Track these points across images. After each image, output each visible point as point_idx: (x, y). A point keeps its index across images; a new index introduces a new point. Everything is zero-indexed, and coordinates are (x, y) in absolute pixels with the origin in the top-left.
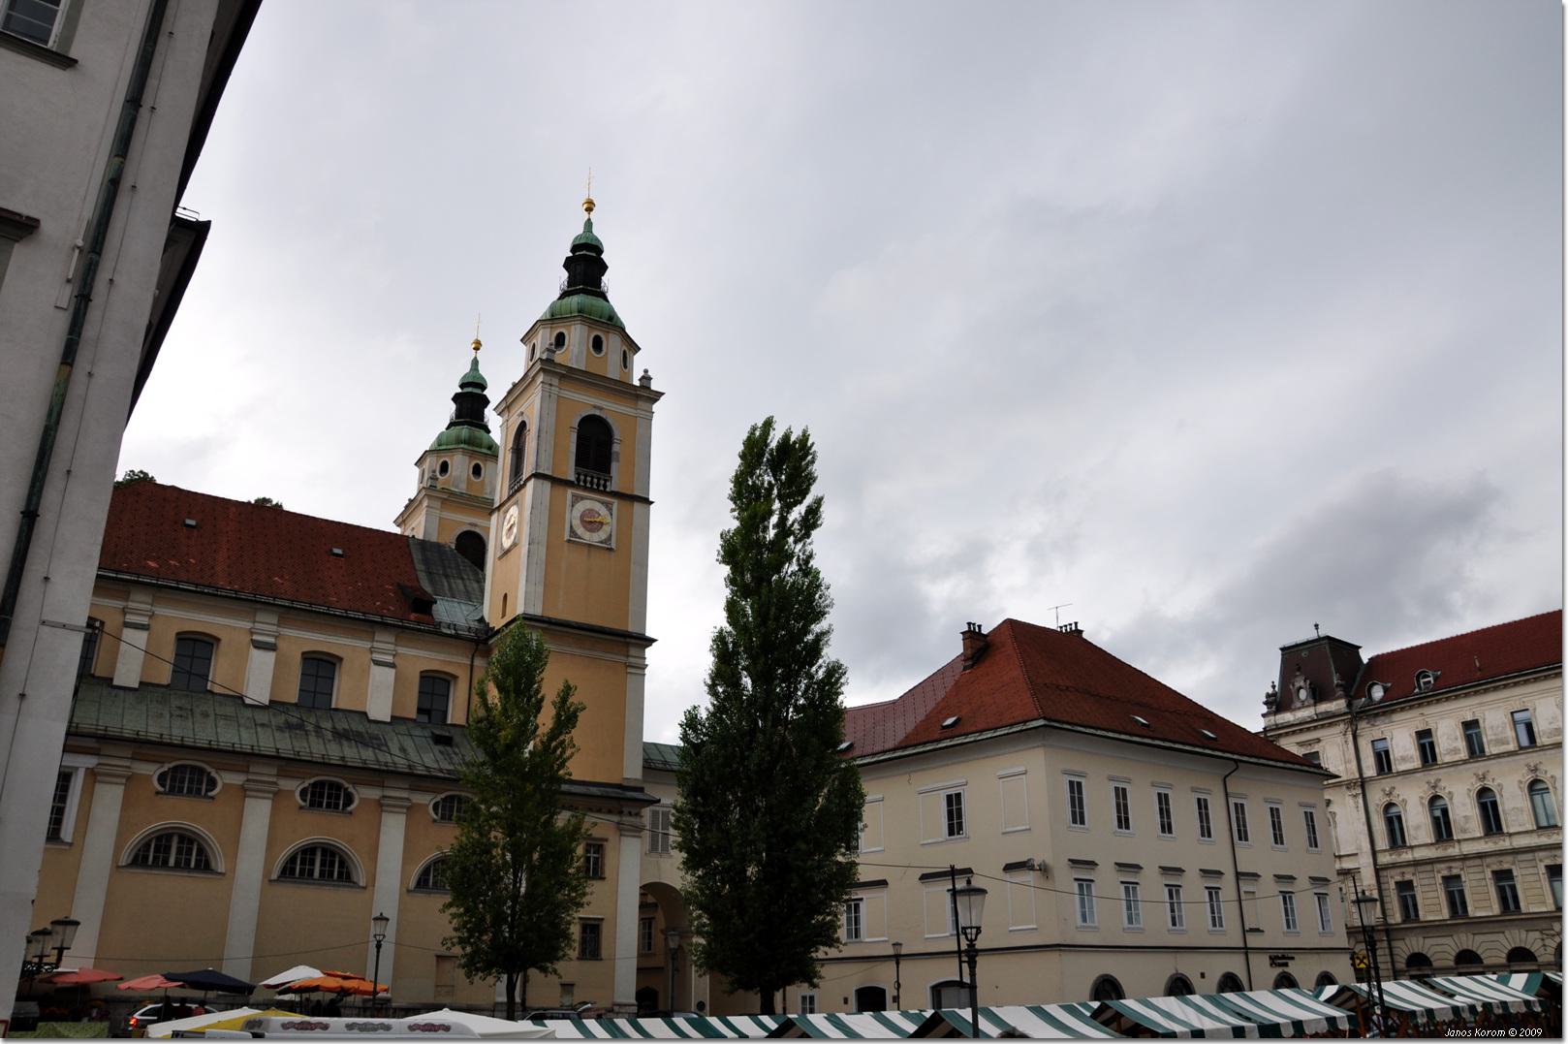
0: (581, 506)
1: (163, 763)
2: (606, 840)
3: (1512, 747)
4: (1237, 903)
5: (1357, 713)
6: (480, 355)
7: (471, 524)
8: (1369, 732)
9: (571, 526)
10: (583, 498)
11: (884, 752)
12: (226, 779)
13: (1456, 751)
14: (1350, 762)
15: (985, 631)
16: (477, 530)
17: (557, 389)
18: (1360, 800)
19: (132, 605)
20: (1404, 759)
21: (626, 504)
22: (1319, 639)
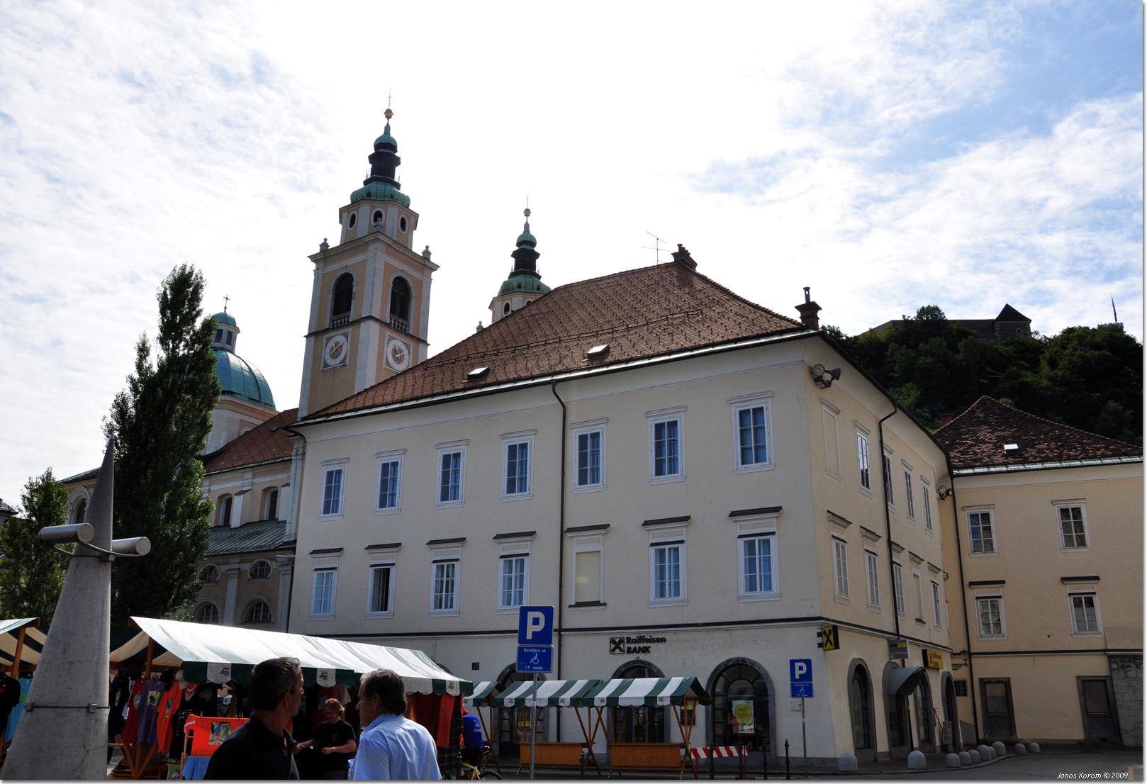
0: (331, 344)
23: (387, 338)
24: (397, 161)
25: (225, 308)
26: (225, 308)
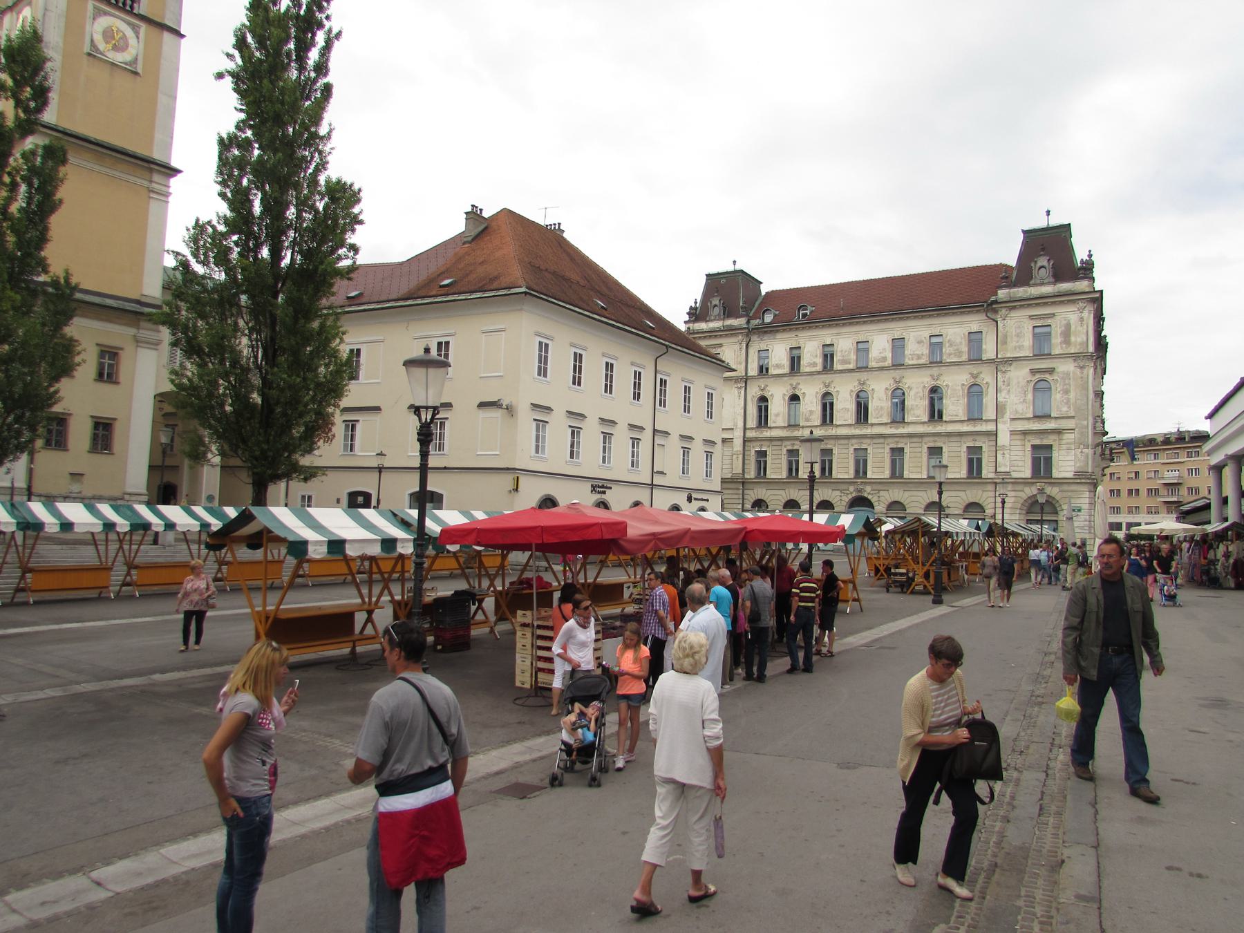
0: (104, 22)
2: (122, 349)
3: (851, 366)
5: (753, 329)
8: (758, 344)
10: (106, 13)
11: (389, 301)
13: (815, 364)
14: (740, 363)
15: (486, 214)
18: (743, 392)
20: (778, 366)
21: (155, 31)
22: (735, 272)
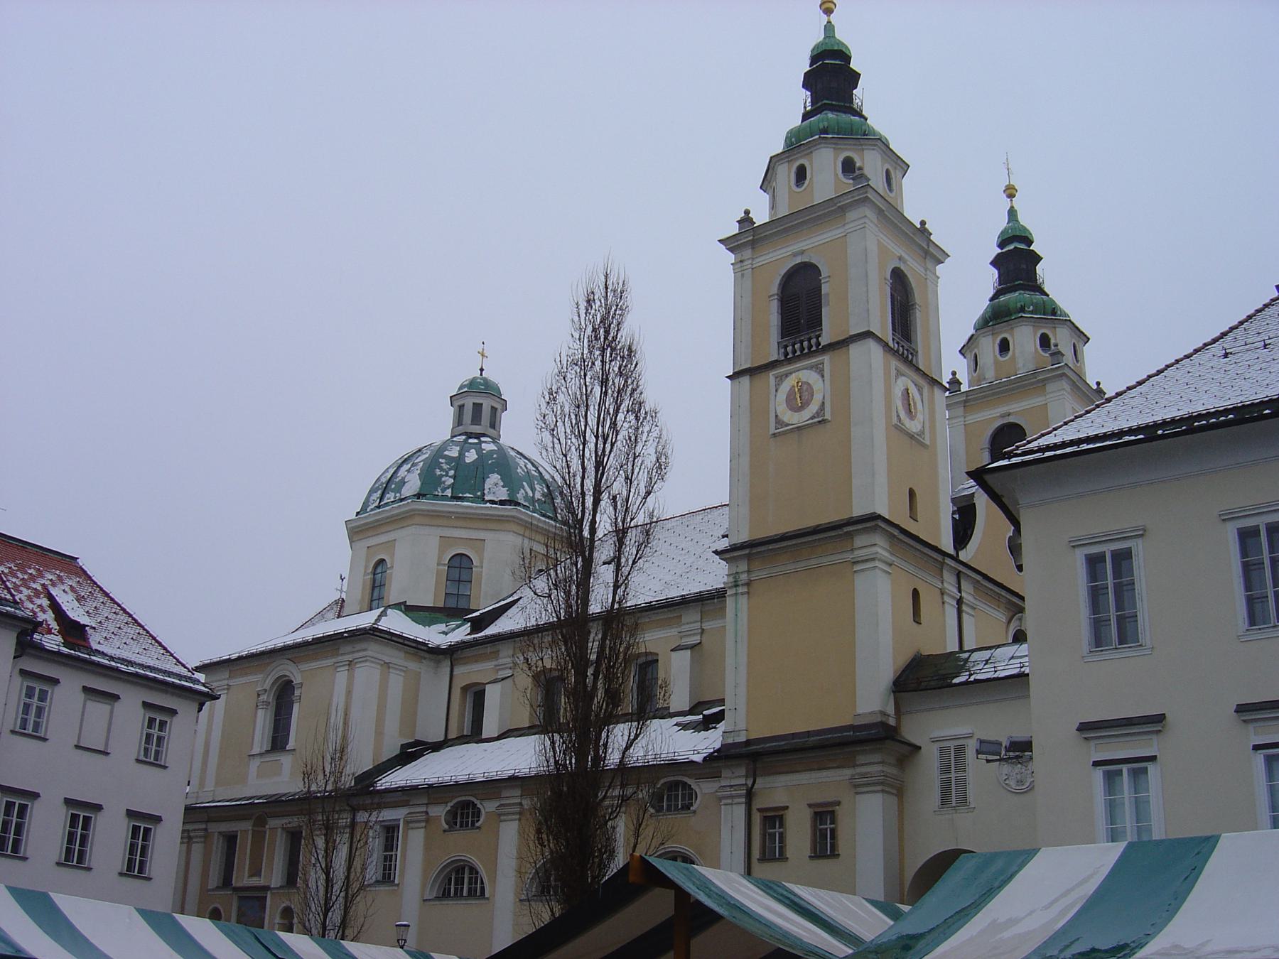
1: (447, 803)
2: (838, 803)
4: (734, 806)
6: (1017, 202)
7: (1002, 416)
9: (776, 416)
10: (787, 376)
12: (488, 807)
16: (1011, 419)
17: (750, 262)
19: (501, 661)
23: (894, 372)
24: (854, 78)
25: (482, 370)
26: (482, 370)
